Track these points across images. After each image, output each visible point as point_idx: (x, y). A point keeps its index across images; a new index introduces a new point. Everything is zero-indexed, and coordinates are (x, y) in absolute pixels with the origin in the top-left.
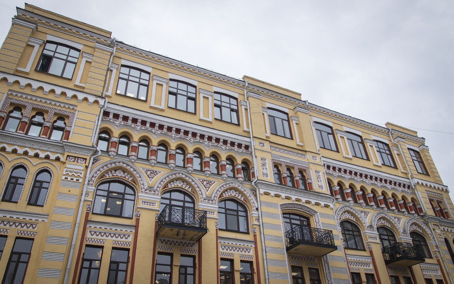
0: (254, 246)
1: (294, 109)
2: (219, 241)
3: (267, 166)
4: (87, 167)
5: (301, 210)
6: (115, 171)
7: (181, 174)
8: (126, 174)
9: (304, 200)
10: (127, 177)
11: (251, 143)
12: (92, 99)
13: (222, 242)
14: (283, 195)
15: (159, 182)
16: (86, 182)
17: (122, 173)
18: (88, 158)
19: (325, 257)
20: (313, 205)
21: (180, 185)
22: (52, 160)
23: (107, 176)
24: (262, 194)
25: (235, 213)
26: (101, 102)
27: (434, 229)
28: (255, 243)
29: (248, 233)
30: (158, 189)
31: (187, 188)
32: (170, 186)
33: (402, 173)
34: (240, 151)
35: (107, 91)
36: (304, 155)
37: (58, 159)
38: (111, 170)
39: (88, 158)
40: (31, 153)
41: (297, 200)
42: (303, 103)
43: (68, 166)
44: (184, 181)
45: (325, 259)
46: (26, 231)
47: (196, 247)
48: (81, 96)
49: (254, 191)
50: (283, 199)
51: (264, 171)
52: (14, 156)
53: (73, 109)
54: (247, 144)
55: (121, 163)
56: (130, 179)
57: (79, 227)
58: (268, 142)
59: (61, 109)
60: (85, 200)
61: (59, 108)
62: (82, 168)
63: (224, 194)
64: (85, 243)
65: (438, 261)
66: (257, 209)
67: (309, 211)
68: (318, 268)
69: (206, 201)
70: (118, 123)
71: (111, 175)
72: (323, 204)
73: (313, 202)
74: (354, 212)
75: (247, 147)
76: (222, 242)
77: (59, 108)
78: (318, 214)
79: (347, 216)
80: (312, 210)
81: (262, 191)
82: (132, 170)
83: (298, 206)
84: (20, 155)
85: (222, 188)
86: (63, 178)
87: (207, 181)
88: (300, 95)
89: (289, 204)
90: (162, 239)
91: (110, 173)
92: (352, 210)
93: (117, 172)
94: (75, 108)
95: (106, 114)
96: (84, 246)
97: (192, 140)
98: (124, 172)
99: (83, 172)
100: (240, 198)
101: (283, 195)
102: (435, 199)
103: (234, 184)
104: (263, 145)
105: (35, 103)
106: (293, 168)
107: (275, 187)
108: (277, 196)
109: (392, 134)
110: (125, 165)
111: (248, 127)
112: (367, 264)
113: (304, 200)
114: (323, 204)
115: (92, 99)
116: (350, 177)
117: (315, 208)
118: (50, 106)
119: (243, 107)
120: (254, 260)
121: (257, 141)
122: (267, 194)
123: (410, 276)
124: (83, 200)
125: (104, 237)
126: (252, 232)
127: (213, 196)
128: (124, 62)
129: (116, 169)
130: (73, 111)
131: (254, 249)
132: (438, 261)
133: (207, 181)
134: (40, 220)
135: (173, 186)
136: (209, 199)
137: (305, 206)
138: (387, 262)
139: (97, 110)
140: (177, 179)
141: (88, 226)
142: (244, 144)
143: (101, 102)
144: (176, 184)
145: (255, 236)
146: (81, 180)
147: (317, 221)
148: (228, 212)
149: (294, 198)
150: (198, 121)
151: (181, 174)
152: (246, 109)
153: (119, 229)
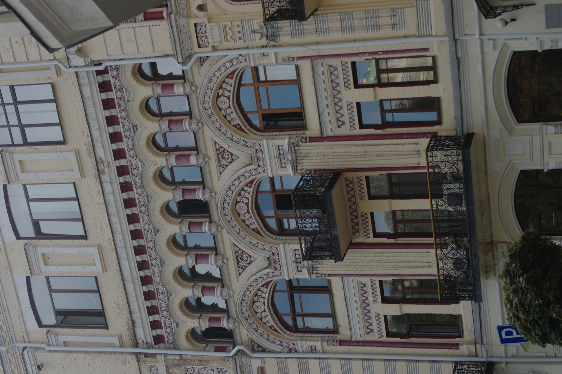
27: (215, 49)
92: (248, 300)
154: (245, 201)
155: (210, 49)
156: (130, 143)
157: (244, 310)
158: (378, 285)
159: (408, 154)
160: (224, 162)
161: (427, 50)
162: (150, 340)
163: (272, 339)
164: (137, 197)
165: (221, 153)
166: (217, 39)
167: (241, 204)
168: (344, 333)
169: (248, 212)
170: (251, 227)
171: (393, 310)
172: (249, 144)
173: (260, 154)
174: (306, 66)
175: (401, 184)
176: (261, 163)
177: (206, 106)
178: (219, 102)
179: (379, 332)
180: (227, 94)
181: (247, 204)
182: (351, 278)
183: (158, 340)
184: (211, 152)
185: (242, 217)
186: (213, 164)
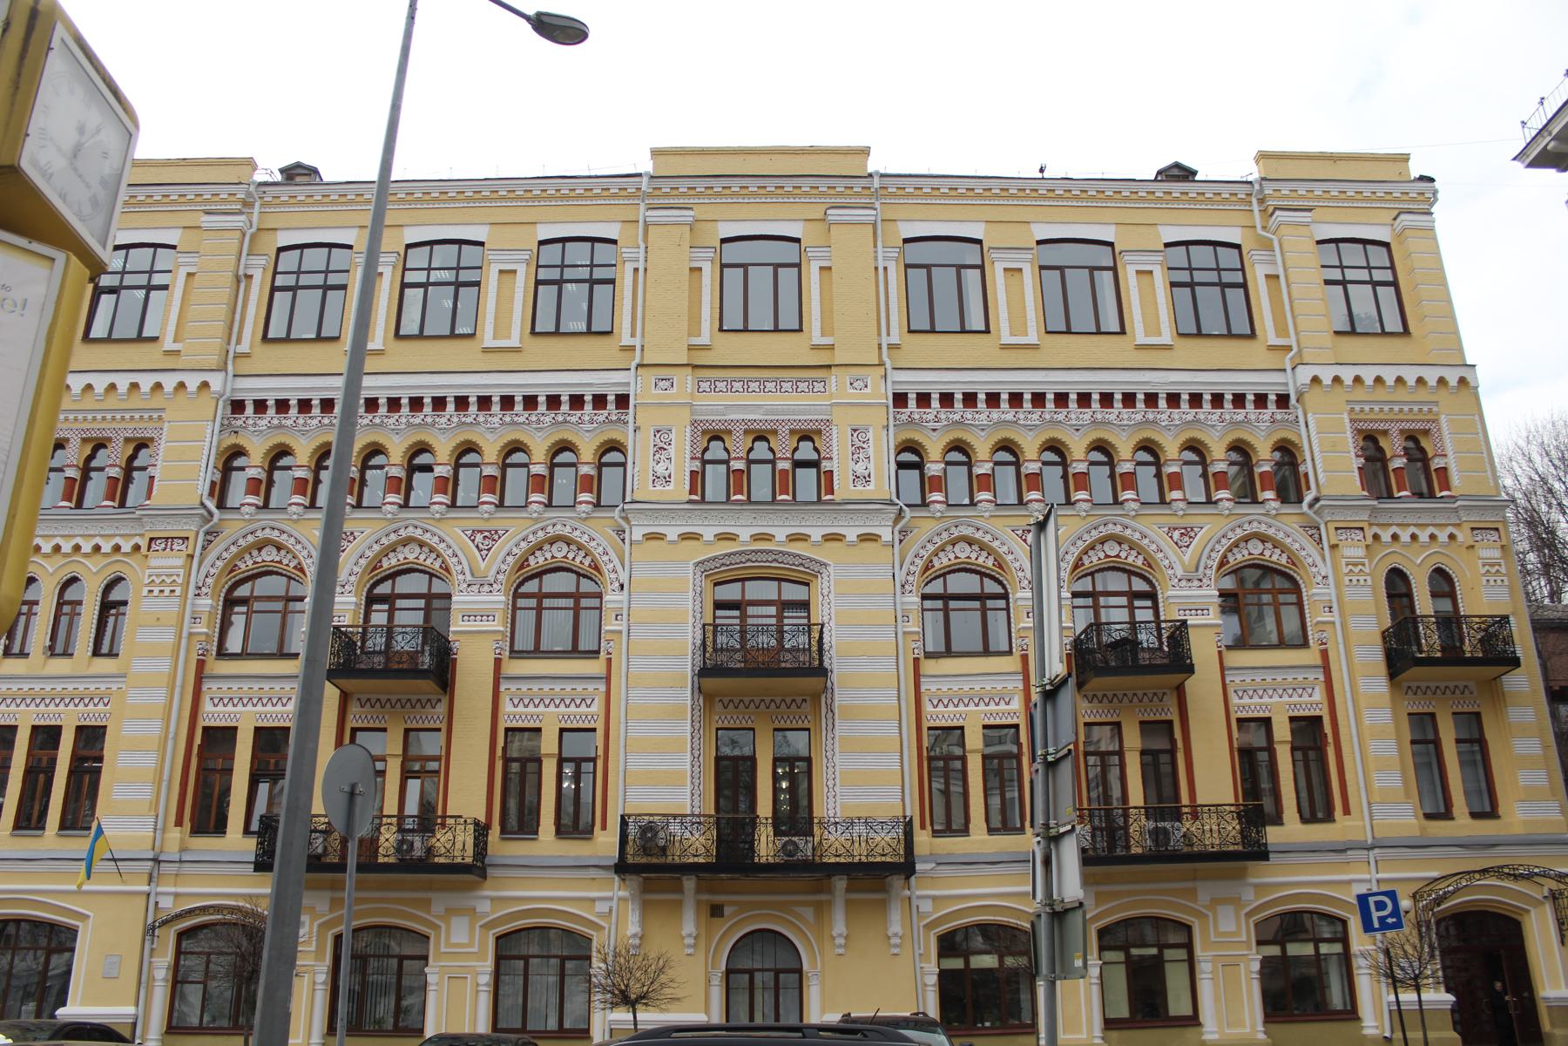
0: (603, 688)
2: (502, 688)
3: (672, 450)
4: (192, 557)
6: (260, 550)
7: (411, 529)
8: (283, 552)
9: (781, 534)
10: (285, 562)
12: (193, 381)
13: (513, 689)
14: (708, 533)
15: (353, 560)
16: (192, 590)
17: (275, 551)
18: (192, 536)
20: (815, 544)
21: (411, 557)
22: (126, 554)
23: (243, 567)
24: (638, 542)
25: (570, 602)
26: (216, 382)
27: (1333, 547)
28: (608, 679)
29: (594, 654)
30: (353, 578)
31: (428, 562)
32: (385, 564)
33: (1272, 348)
34: (601, 418)
35: (239, 342)
37: (137, 548)
38: (248, 550)
39: (192, 536)
40: (87, 547)
41: (757, 538)
42: (864, 182)
43: (153, 562)
44: (422, 545)
46: (90, 714)
47: (442, 709)
48: (169, 381)
50: (708, 543)
51: (660, 469)
52: (59, 560)
56: (292, 565)
57: (182, 694)
58: (689, 370)
59: (137, 425)
60: (191, 634)
61: (132, 425)
62: (180, 562)
63: (531, 558)
64: (201, 723)
65: (1325, 654)
66: (622, 586)
69: (475, 588)
70: (265, 422)
71: (250, 563)
72: (851, 534)
73: (816, 534)
74: (988, 538)
75: (623, 401)
76: (513, 689)
77: (132, 425)
78: (830, 569)
79: (963, 556)
80: (811, 560)
81: (638, 534)
83: (764, 557)
84: (66, 555)
85: (523, 544)
86: (145, 592)
87: (481, 532)
88: (865, 152)
89: (729, 555)
90: (364, 697)
91: (247, 557)
92: (978, 535)
93: (264, 552)
95: (238, 406)
96: (199, 733)
97: (455, 419)
98: (279, 549)
99: (182, 572)
100: (579, 561)
101: (708, 533)
102: (1394, 429)
103: (559, 527)
104: (667, 384)
105: (85, 426)
106: (775, 432)
108: (686, 537)
109: (1261, 201)
110: (276, 533)
111: (633, 335)
112: (1004, 698)
113: (781, 534)
114: (851, 534)
115: (193, 381)
116: (1010, 417)
118: (114, 425)
119: (629, 267)
121: (650, 375)
122: (651, 537)
123: (1174, 716)
124: (185, 634)
125: (240, 708)
127: (493, 572)
128: (285, 239)
129: (260, 546)
130: (157, 425)
131: (603, 696)
132: (1325, 654)
133: (481, 532)
134: (114, 687)
135: (394, 562)
136: (479, 582)
137: (789, 554)
139: (206, 406)
140: (406, 542)
141: (205, 688)
143: (216, 382)
144: (401, 557)
146: (178, 591)
147: (825, 592)
148: (547, 603)
149: (745, 534)
150: (481, 356)
151: (411, 529)
152: (636, 270)
153: (266, 686)
154: (1123, 555)
155: (1333, 542)
156: (1190, 417)
157: (961, 528)
158: (1009, 721)
159: (1213, 778)
160: (1176, 535)
161: (1347, 811)
162: (901, 389)
163: (918, 561)
164: (1116, 411)
165: (1188, 532)
166: (1348, 552)
167: (1117, 548)
168: (929, 667)
169: (1107, 556)
170: (1085, 558)
171: (974, 740)
172: (1208, 572)
173: (1196, 583)
174: (1310, 656)
175: (1164, 766)
176: (1183, 583)
177: (1255, 524)
178: (1255, 541)
179: (939, 715)
180: (1267, 553)
181: (1118, 556)
182: (1021, 686)
183: (900, 399)
184: (1187, 522)
185: (1098, 547)
186: (1174, 521)
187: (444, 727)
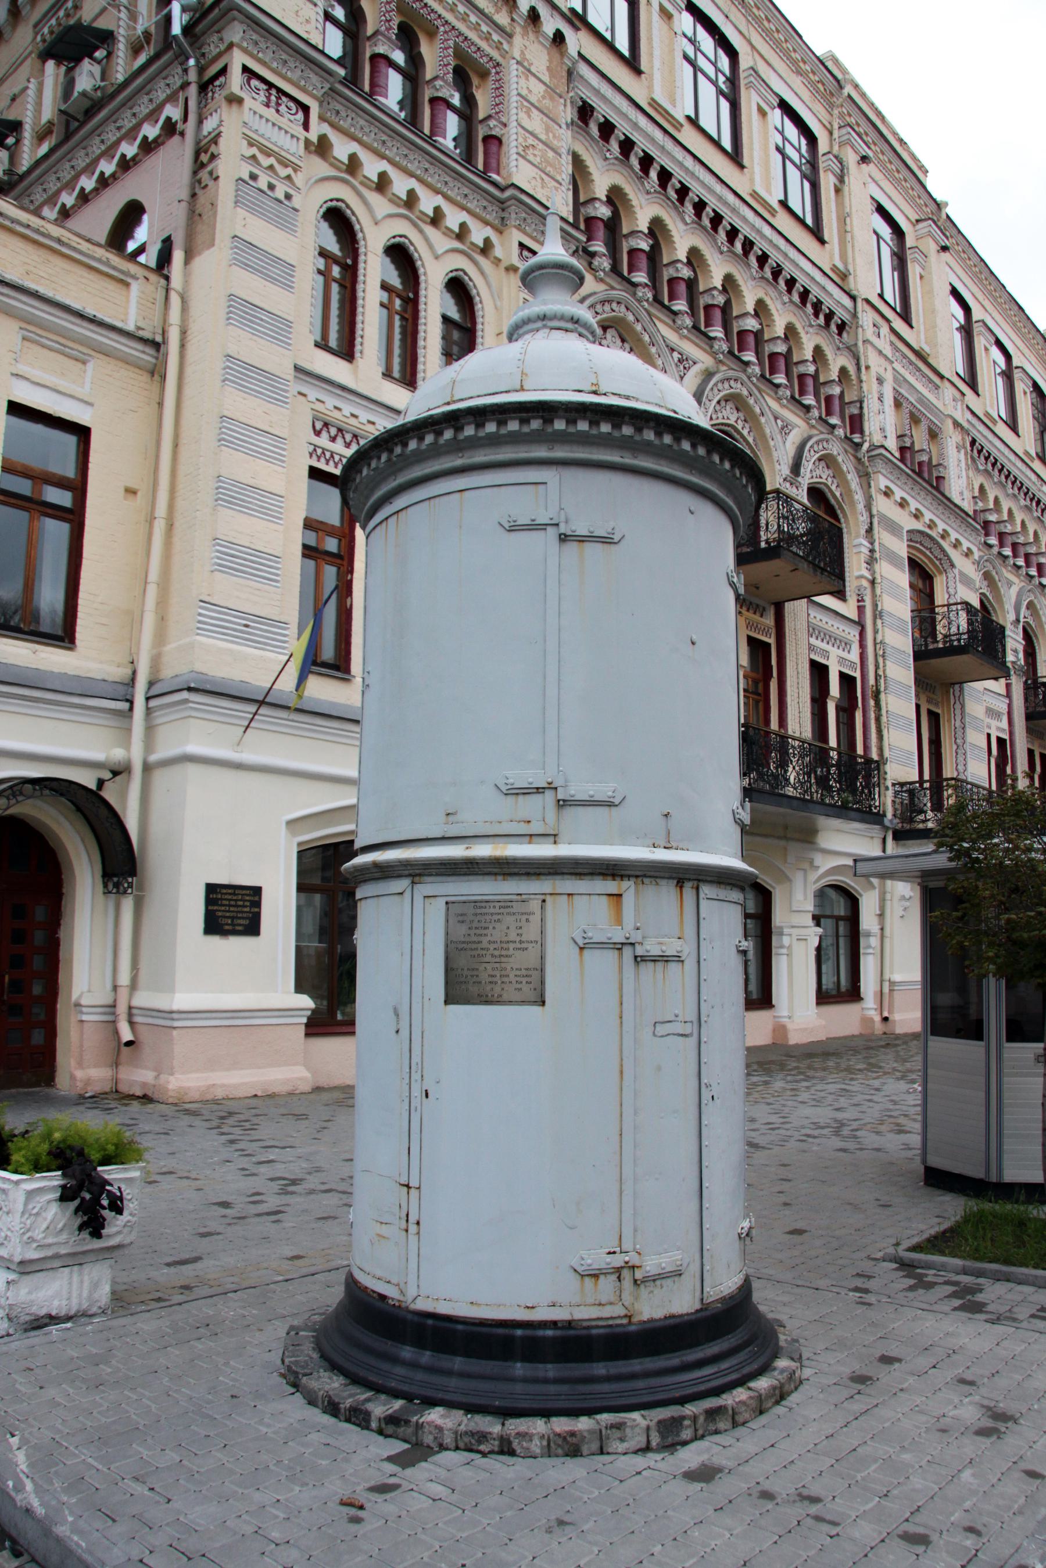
1: (917, 221)
5: (928, 553)
11: (855, 315)
12: (550, 24)
19: (957, 687)
36: (937, 387)
45: (957, 694)
47: (769, 621)
49: (865, 476)
53: (498, 46)
54: (846, 317)
55: (623, 309)
67: (940, 560)
68: (939, 711)
78: (956, 571)
80: (949, 559)
81: (882, 482)
82: (646, 338)
94: (506, 46)
107: (904, 477)
108: (903, 504)
113: (941, 526)
115: (550, 24)
117: (954, 555)
120: (857, 675)
122: (888, 493)
126: (855, 598)
138: (1029, 717)
142: (841, 314)
145: (861, 609)
187: (772, 641)
